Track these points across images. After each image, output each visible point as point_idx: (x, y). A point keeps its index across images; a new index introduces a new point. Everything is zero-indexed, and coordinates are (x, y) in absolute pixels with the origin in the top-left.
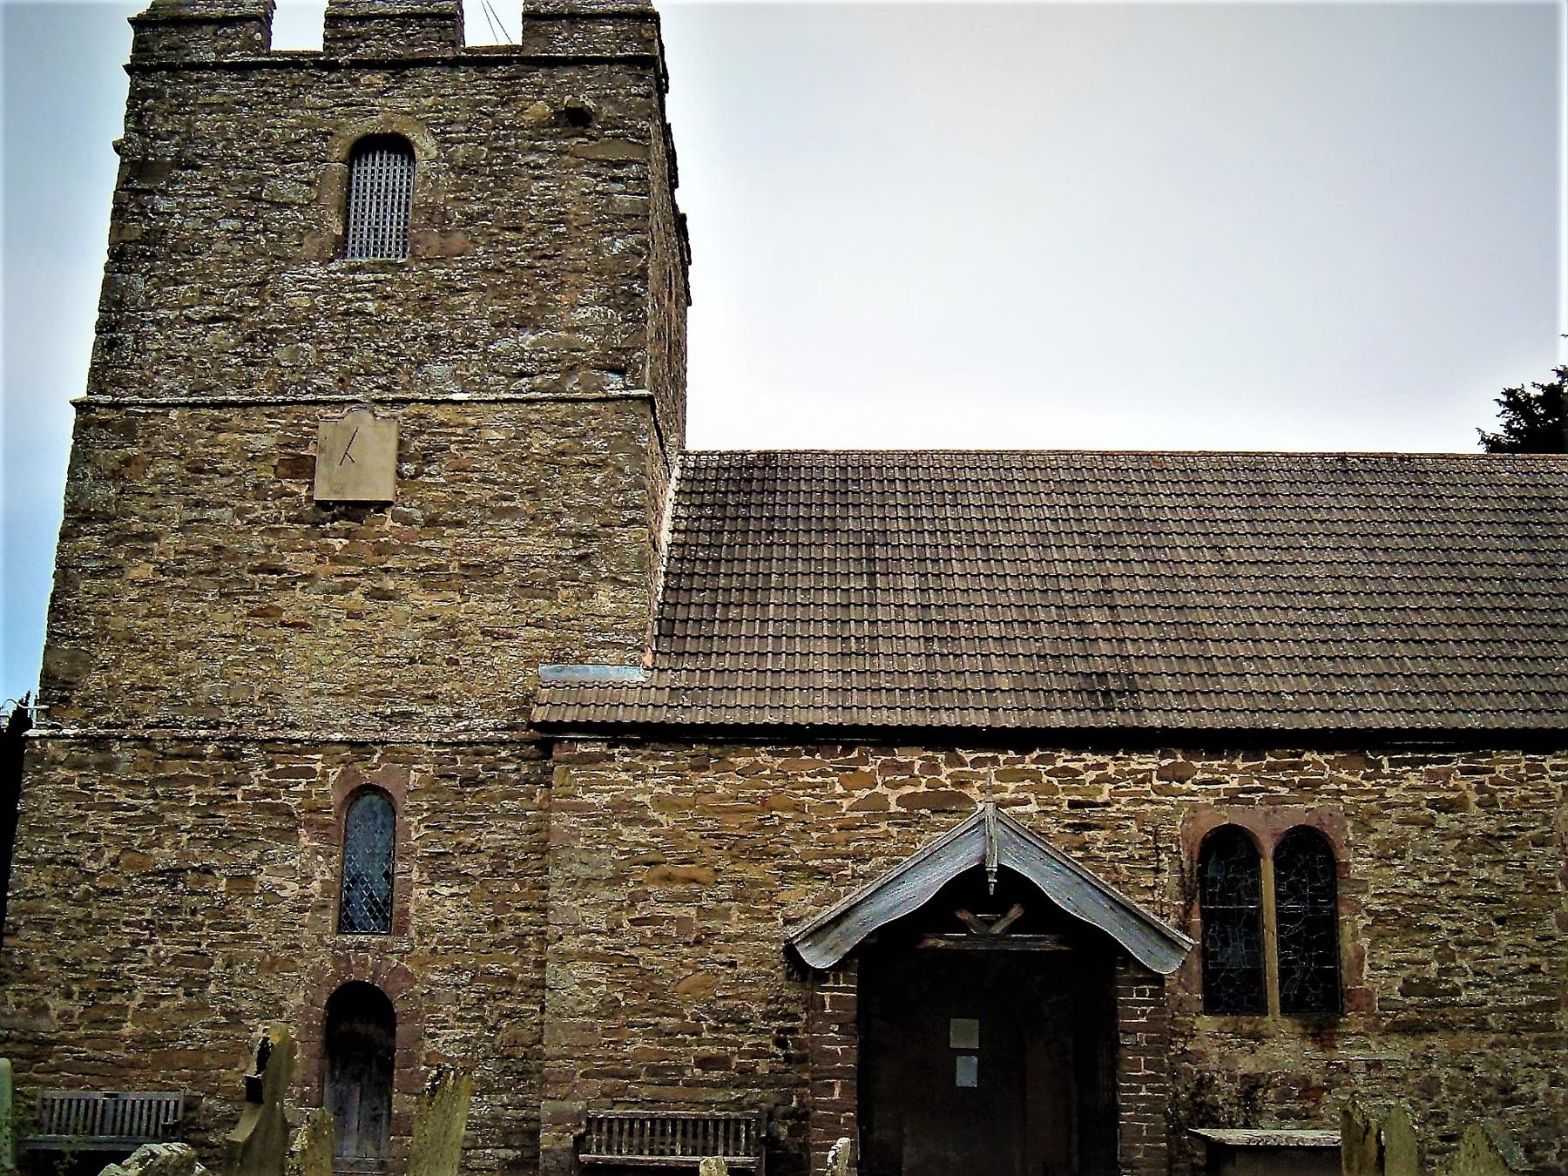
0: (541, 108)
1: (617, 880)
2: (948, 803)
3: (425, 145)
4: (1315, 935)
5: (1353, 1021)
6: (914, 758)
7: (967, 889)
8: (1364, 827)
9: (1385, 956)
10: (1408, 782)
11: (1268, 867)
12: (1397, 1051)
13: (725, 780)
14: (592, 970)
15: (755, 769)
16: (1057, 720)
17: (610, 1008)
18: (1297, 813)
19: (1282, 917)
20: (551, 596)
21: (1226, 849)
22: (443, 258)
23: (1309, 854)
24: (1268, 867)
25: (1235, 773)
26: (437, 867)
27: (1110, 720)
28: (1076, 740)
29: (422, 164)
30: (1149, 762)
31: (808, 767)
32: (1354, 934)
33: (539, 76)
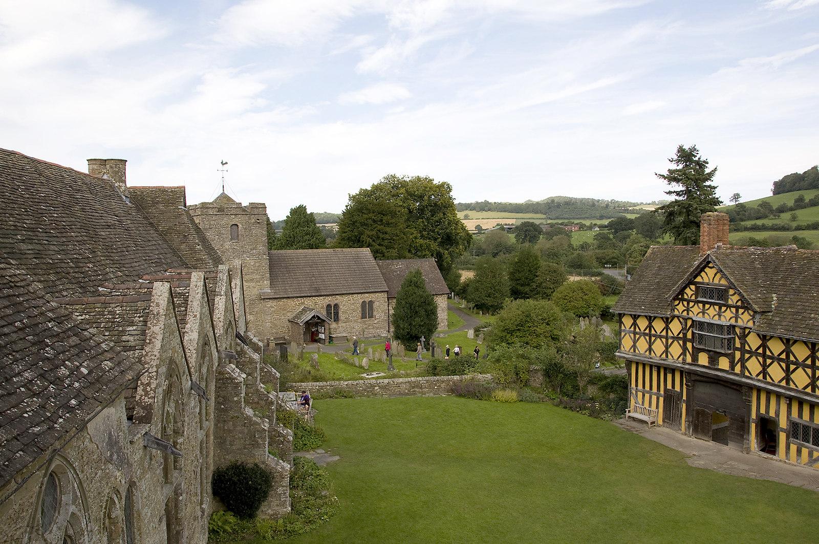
0: (253, 221)
1: (271, 314)
2: (303, 303)
3: (240, 226)
4: (336, 314)
5: (340, 322)
6: (300, 299)
7: (314, 317)
8: (342, 303)
9: (343, 316)
10: (346, 298)
11: (333, 307)
12: (344, 325)
13: (281, 303)
14: (269, 323)
15: (284, 302)
16: (314, 294)
17: (271, 327)
18: (336, 302)
19: (334, 312)
20: (259, 282)
21: (329, 306)
22: (244, 240)
23: (336, 306)
24: (333, 307)
25: (330, 298)
26: (250, 314)
27: (317, 294)
28: (315, 296)
29: (240, 229)
30: (322, 298)
31: (289, 301)
32: (340, 313)
33: (253, 216)
